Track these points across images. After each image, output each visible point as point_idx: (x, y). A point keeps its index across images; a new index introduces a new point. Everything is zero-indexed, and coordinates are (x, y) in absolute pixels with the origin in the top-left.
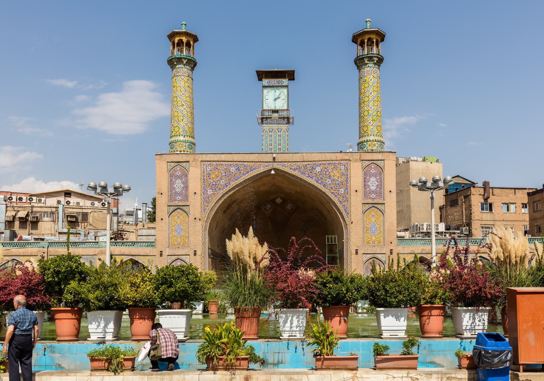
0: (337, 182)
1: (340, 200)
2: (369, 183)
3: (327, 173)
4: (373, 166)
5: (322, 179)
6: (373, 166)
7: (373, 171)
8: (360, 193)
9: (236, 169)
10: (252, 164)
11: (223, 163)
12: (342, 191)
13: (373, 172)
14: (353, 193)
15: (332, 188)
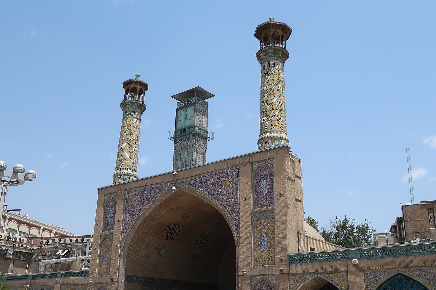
0: (228, 192)
1: (231, 212)
2: (260, 188)
3: (220, 183)
4: (264, 167)
5: (214, 190)
6: (264, 167)
7: (264, 173)
8: (250, 201)
9: (148, 193)
10: (160, 185)
11: (139, 189)
12: (232, 201)
13: (263, 174)
14: (242, 202)
15: (223, 199)
